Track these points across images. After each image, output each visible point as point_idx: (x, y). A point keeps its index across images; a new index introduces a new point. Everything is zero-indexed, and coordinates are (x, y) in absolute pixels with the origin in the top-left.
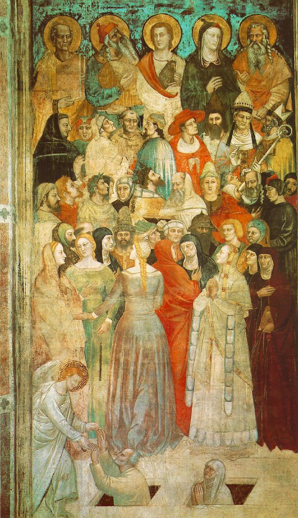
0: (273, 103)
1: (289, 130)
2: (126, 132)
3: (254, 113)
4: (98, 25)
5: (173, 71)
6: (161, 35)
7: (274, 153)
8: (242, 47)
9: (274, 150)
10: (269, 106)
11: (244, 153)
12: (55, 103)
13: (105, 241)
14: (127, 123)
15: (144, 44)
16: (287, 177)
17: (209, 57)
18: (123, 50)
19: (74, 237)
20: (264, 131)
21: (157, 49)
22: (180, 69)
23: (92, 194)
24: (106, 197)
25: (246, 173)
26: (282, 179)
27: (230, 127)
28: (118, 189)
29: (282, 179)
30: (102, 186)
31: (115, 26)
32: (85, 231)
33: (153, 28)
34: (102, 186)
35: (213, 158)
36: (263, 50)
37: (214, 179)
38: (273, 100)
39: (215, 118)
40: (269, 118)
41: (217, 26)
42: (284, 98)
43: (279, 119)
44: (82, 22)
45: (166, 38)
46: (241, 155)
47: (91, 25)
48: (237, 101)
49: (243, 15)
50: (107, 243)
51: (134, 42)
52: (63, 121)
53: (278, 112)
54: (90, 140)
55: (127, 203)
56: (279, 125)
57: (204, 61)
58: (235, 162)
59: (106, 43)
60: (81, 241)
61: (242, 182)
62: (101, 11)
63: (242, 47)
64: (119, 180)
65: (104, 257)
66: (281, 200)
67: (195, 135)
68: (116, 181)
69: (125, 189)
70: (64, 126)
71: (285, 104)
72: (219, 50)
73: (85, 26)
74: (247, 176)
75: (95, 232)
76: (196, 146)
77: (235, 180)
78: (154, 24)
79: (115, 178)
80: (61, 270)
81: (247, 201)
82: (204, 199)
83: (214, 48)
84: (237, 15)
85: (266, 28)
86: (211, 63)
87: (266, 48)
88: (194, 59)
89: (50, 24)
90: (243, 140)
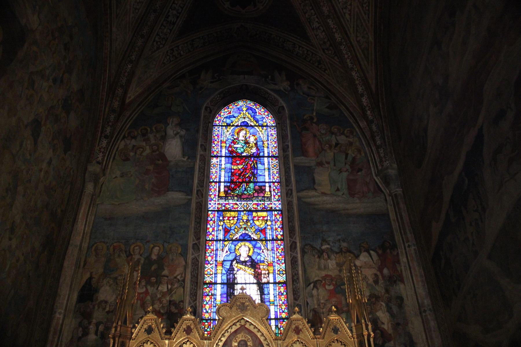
0: (177, 274)
1: (182, 284)
2: (117, 284)
3: (169, 278)
4: (113, 246)
5: (139, 262)
6: (137, 249)
7: (175, 293)
8: (167, 254)
9: (176, 291)
10: (175, 275)
11: (163, 293)
12: (91, 273)
13: (100, 327)
14: (118, 281)
15: (130, 252)
16: (179, 302)
17: (154, 257)
18: (121, 254)
19: (88, 325)
20: (172, 284)
21: (134, 254)
22: (142, 262)
23: (99, 307)
24: (104, 309)
25: (163, 300)
26: (178, 303)
27: (158, 283)
28: (110, 306)
29: (178, 303)
30: (103, 304)
31: (120, 246)
32: (92, 323)
33: (134, 247)
34: (103, 304)
35: (150, 294)
36: (175, 255)
37: (150, 302)
38: (177, 273)
39: (153, 279)
40: (175, 279)
41: (159, 246)
42: (182, 272)
43: (178, 280)
44: (108, 244)
45: (138, 251)
46: (162, 293)
47: (111, 246)
48: (163, 273)
49: (169, 243)
50: (101, 328)
51: (126, 252)
52: (94, 279)
53: (179, 277)
54: (102, 287)
55: (112, 312)
56: (178, 282)
57: (152, 259)
58: (159, 296)
59: (115, 252)
60: (91, 327)
61: (161, 304)
62: (115, 241)
63: (167, 254)
64: (111, 302)
65: (99, 334)
66: (176, 311)
67: (145, 286)
68: (109, 302)
69: (113, 306)
70: (94, 281)
71: (182, 274)
72: (158, 255)
73: (108, 246)
74: (163, 301)
75: (96, 323)
76: (144, 290)
77: (158, 303)
78: (135, 245)
79: (109, 302)
80: (79, 339)
81: (162, 311)
82: (144, 310)
83: (156, 254)
84: (167, 243)
85: (177, 247)
86: (155, 260)
87: (177, 254)
88: (148, 258)
89: (95, 245)
90: (164, 288)
